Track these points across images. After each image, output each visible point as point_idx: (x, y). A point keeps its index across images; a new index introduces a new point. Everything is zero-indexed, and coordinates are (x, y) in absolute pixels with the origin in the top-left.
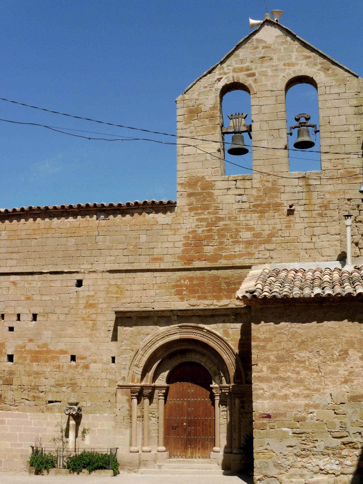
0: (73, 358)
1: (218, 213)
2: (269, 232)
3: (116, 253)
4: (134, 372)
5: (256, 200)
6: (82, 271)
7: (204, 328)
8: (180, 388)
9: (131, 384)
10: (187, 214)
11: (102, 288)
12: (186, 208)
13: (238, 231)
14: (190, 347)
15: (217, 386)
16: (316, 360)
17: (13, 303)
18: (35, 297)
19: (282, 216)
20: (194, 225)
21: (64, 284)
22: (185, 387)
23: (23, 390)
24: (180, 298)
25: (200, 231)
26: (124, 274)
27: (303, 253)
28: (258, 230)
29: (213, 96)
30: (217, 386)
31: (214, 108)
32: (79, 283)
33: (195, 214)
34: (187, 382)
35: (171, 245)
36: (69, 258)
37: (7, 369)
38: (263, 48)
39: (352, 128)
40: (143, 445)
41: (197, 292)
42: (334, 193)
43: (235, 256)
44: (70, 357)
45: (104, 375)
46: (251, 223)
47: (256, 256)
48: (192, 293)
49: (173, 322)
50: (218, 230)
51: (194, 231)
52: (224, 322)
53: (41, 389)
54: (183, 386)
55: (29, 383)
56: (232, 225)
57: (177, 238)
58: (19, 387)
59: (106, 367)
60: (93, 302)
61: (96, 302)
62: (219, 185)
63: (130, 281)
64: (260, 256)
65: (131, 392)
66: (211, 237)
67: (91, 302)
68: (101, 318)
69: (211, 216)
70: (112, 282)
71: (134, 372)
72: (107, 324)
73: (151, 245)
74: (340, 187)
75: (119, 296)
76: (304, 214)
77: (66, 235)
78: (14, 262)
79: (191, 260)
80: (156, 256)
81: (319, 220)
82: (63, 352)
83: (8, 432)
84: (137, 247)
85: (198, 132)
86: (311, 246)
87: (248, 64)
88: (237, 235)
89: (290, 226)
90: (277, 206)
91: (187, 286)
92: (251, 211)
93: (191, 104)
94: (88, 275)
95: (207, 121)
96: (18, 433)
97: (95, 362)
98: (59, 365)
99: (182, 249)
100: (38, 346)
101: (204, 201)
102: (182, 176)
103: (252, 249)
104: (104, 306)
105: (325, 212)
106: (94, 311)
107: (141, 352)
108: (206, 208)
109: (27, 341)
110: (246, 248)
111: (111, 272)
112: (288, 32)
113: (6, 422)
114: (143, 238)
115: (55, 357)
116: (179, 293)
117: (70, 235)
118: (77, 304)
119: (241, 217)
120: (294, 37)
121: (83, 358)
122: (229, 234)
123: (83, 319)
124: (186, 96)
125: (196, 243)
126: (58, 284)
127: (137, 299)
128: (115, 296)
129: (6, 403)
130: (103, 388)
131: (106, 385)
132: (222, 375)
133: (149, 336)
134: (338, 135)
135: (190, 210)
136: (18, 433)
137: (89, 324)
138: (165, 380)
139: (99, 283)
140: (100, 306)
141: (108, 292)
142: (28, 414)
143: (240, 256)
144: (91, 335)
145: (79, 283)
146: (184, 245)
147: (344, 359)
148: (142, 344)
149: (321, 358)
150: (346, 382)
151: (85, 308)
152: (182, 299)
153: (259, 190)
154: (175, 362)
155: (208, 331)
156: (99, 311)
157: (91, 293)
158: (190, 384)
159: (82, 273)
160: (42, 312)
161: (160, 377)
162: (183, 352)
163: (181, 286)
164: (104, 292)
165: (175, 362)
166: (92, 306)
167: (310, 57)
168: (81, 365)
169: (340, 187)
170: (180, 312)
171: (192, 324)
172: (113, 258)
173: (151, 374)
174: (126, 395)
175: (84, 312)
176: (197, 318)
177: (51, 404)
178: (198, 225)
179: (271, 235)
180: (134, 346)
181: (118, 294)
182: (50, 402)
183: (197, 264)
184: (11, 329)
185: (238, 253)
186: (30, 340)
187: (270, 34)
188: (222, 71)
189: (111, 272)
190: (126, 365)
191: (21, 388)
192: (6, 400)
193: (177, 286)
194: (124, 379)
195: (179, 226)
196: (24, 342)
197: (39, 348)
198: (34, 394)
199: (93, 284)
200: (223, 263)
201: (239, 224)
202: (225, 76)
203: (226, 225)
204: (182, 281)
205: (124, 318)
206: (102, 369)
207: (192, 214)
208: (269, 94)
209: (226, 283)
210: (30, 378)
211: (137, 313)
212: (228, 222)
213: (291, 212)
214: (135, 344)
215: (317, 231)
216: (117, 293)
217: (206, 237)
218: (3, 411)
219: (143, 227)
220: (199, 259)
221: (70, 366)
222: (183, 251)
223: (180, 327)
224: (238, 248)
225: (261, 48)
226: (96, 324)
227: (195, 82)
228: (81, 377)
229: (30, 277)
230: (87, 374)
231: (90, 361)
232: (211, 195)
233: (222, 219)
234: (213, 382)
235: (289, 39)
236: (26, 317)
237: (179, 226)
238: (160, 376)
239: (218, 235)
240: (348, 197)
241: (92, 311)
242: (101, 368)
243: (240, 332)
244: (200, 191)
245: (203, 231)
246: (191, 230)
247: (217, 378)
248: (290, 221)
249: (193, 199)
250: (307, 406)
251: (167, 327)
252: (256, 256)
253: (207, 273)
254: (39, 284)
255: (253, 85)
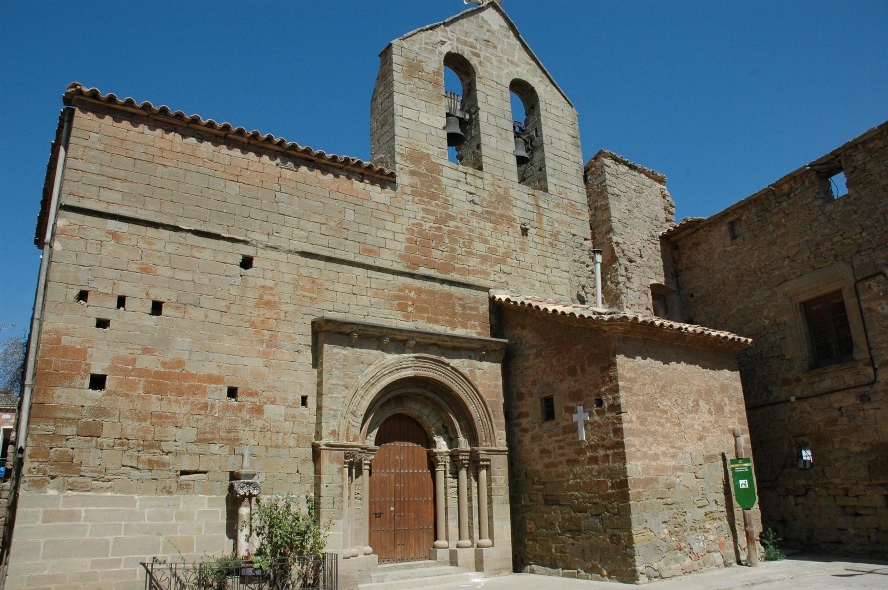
0: (232, 392)
1: (448, 208)
2: (504, 250)
3: (310, 226)
4: (349, 422)
5: (489, 206)
6: (254, 242)
7: (448, 365)
9: (345, 443)
10: (411, 198)
11: (287, 278)
12: (409, 190)
13: (471, 240)
14: (418, 391)
16: (675, 411)
17: (111, 274)
18: (160, 270)
19: (516, 235)
20: (419, 216)
21: (220, 257)
23: (125, 448)
24: (404, 316)
25: (427, 226)
26: (322, 264)
27: (537, 284)
28: (493, 244)
29: (436, 58)
31: (436, 73)
32: (247, 263)
33: (420, 200)
35: (390, 235)
36: (229, 216)
37: (88, 404)
38: (488, 30)
39: (571, 157)
40: (345, 547)
41: (426, 310)
42: (561, 223)
43: (469, 272)
44: (226, 390)
45: (288, 426)
46: (486, 233)
47: (492, 277)
48: (419, 312)
50: (448, 231)
51: (419, 225)
52: (470, 358)
53: (165, 446)
55: (141, 434)
56: (464, 229)
57: (397, 227)
58: (118, 441)
59: (292, 411)
60: (272, 298)
61: (276, 299)
62: (447, 172)
63: (333, 275)
64: (497, 279)
65: (346, 457)
66: (440, 239)
67: (267, 298)
68: (285, 329)
69: (440, 210)
70: (304, 272)
71: (349, 422)
72: (295, 339)
73: (364, 229)
74: (566, 218)
75: (315, 296)
76: (537, 239)
77: (224, 176)
78: (117, 197)
79: (417, 265)
80: (369, 247)
81: (550, 250)
82: (217, 380)
83: (87, 536)
84: (341, 225)
85: (419, 94)
86: (544, 278)
87: (472, 40)
88: (471, 244)
89: (524, 250)
90: (511, 220)
91: (412, 299)
92: (484, 218)
93: (412, 55)
94: (262, 251)
95: (430, 87)
96: (111, 538)
97: (273, 402)
98: (207, 403)
99: (404, 245)
100: (164, 364)
101: (431, 187)
102: (401, 144)
103: (486, 267)
104: (290, 308)
105: (555, 242)
106: (272, 314)
107: (361, 392)
108: (434, 197)
109: (140, 352)
110: (482, 263)
111: (304, 254)
112: (512, 27)
113: (83, 515)
114: (350, 215)
115: (198, 388)
116: (402, 308)
117: (231, 177)
118: (243, 297)
119: (474, 221)
120: (517, 35)
121: (251, 394)
122: (461, 240)
123: (253, 325)
124: (405, 44)
125: (421, 241)
126: (207, 255)
127: (343, 306)
128: (309, 295)
129: (82, 474)
130: (287, 450)
131: (292, 443)
133: (372, 367)
134: (562, 161)
135: (414, 193)
136: (111, 538)
137: (263, 335)
139: (282, 268)
140: (284, 307)
141: (296, 287)
142: (136, 497)
143: (475, 272)
144: (265, 354)
145: (247, 263)
146: (407, 239)
147: (696, 411)
148: (362, 380)
149: (679, 409)
150: (700, 439)
151: (257, 306)
152: (407, 318)
153: (490, 194)
155: (452, 368)
156: (282, 316)
157: (269, 283)
159: (253, 245)
160: (174, 300)
163: (407, 298)
164: (291, 286)
165: (389, 413)
166: (269, 304)
167: (530, 64)
168: (248, 405)
169: (566, 218)
171: (434, 357)
172: (304, 234)
174: (338, 462)
175: (256, 313)
176: (436, 348)
177: (184, 477)
178: (424, 217)
179: (507, 255)
180: (349, 380)
181: (313, 293)
182: (184, 473)
183: (423, 270)
184: (102, 324)
185: (472, 268)
186: (146, 351)
187: (491, 17)
188: (445, 34)
189: (304, 254)
190: (337, 410)
191: (122, 444)
192: (82, 468)
193: (399, 297)
194: (334, 433)
195: (399, 212)
196: (132, 352)
197: (164, 367)
198: (149, 456)
199: (272, 268)
200: (456, 277)
201: (472, 231)
202: (449, 42)
203: (457, 227)
204: (407, 291)
205: (327, 332)
206: (286, 415)
207: (417, 199)
208: (494, 85)
209: (461, 305)
210: (143, 424)
211: (364, 328)
212: (460, 225)
213: (525, 232)
214: (351, 378)
215: (550, 262)
216: (311, 290)
217: (435, 237)
218: (76, 493)
219: (350, 199)
220: (426, 265)
221: (227, 408)
222: (407, 248)
223: (417, 358)
224: (473, 262)
225: (485, 29)
226: (276, 337)
227: (415, 31)
228: (248, 428)
229: (151, 232)
230: (258, 423)
231: (265, 400)
232: (439, 182)
233: (453, 218)
235: (511, 33)
236: (139, 306)
237: (399, 212)
239: (449, 237)
240: (573, 231)
241: (269, 313)
242: (283, 414)
244: (424, 172)
245: (431, 227)
246: (415, 221)
248: (524, 242)
249: (416, 180)
250: (675, 468)
251: (397, 356)
252: (492, 277)
253: (437, 286)
254: (170, 248)
255: (479, 68)
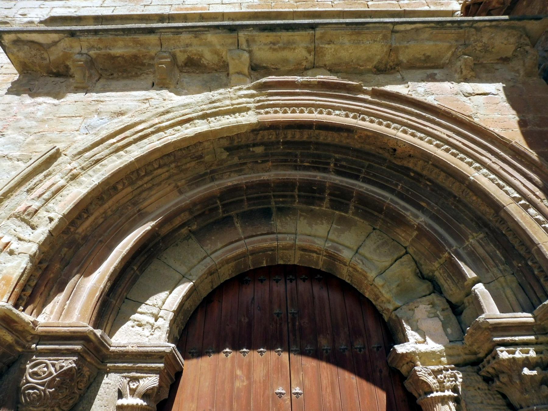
8: (233, 377)
15: (432, 346)
22: (259, 373)
30: (432, 346)
34: (271, 347)
49: (234, 78)
54: (249, 369)
107: (64, 165)
132: (470, 274)
138: (164, 324)
154: (221, 252)
158: (285, 356)
161: (144, 313)
162: (259, 205)
165: (221, 252)
170: (264, 38)
173: (91, 285)
234: (410, 332)
238: (143, 308)
243: (507, 105)
247: (422, 310)
